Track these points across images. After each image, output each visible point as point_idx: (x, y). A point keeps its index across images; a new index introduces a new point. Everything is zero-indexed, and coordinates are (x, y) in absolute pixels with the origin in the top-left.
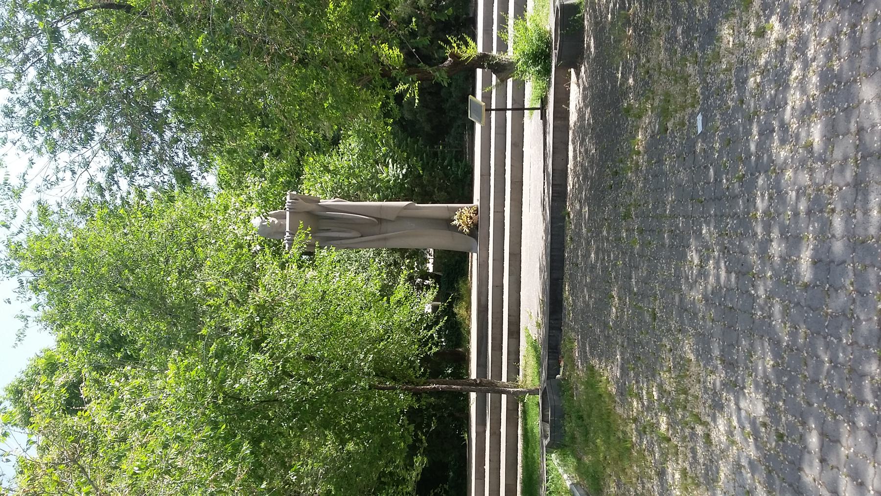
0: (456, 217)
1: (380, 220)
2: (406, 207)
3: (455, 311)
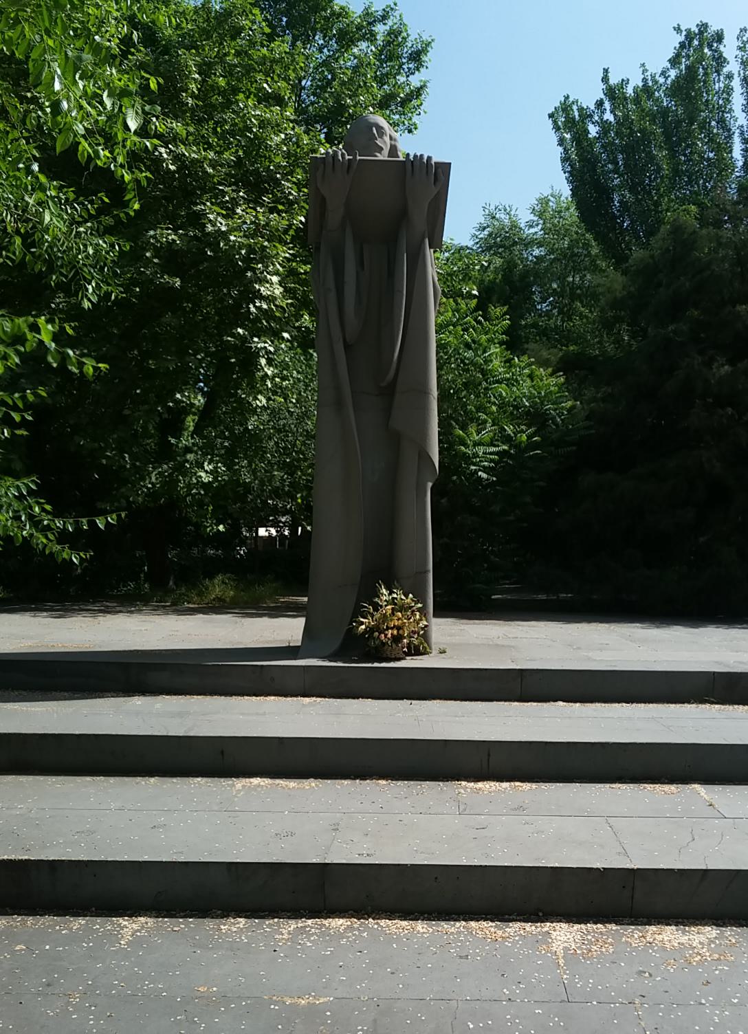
0: (398, 595)
1: (389, 392)
2: (424, 456)
3: (220, 577)
